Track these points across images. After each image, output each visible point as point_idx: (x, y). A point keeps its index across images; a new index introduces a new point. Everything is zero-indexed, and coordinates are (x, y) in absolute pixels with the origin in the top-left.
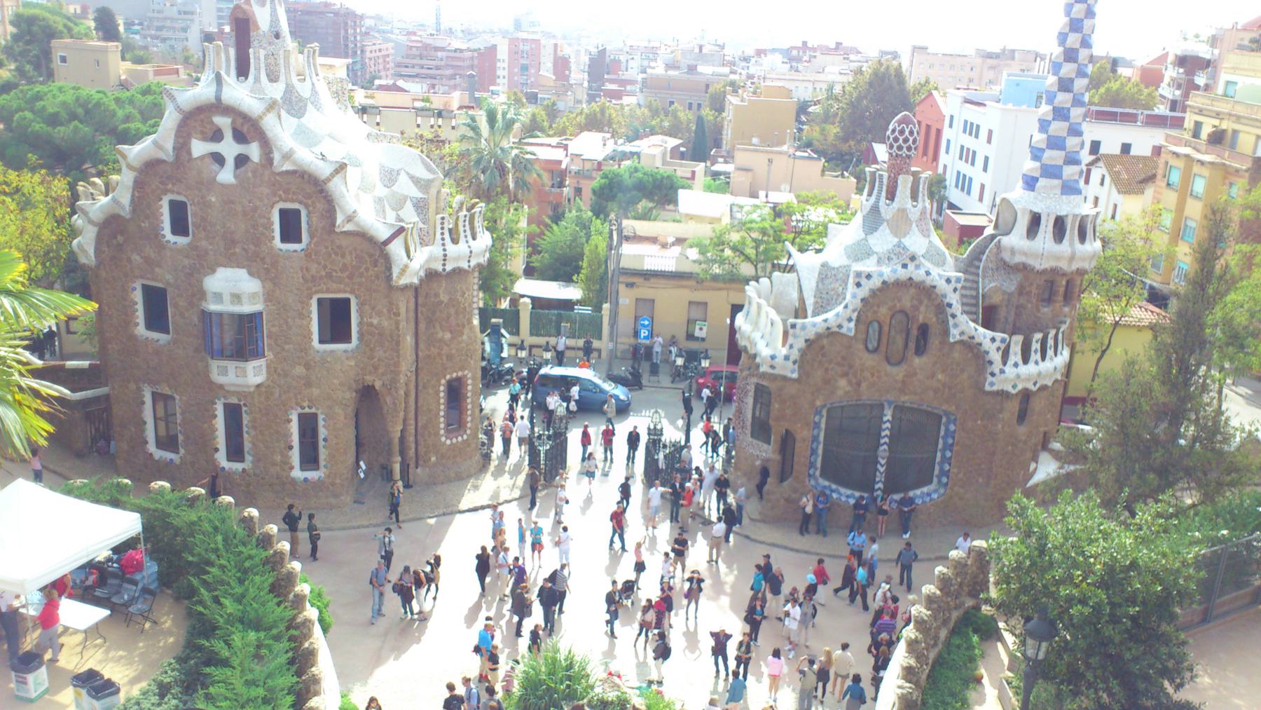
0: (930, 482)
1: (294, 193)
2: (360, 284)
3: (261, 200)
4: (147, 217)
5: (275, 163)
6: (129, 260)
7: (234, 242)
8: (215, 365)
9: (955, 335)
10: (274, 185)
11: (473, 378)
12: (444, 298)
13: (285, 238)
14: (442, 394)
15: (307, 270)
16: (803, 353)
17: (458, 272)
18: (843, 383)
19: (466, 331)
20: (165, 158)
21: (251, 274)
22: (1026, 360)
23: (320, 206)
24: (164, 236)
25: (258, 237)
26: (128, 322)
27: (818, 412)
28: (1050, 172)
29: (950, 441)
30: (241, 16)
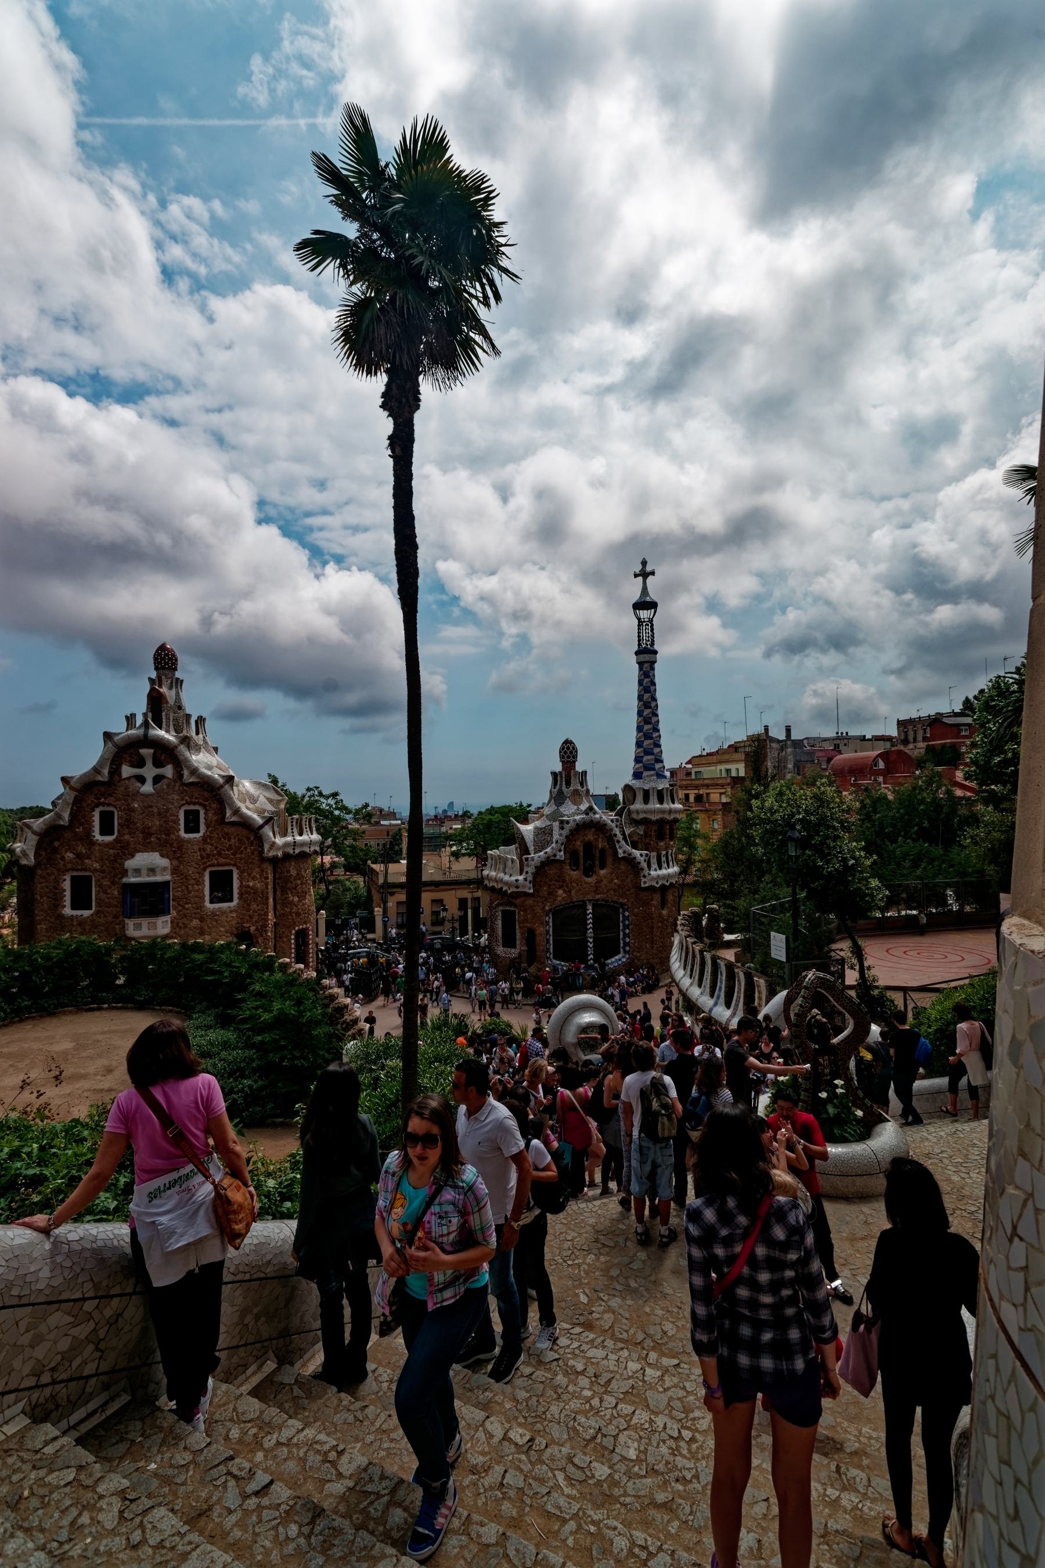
0: (619, 953)
2: (241, 859)
3: (172, 804)
4: (82, 824)
6: (63, 858)
8: (130, 923)
9: (621, 854)
12: (293, 872)
13: (186, 832)
15: (204, 850)
16: (535, 875)
18: (560, 892)
20: (101, 779)
21: (162, 856)
22: (660, 868)
25: (169, 829)
27: (547, 915)
28: (647, 768)
29: (627, 922)
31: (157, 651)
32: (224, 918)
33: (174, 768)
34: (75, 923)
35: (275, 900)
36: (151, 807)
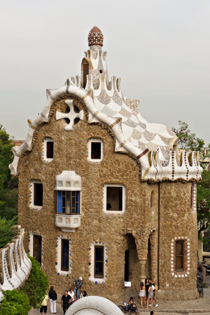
1: (98, 134)
2: (127, 179)
3: (83, 138)
4: (37, 150)
5: (89, 119)
7: (70, 158)
10: (89, 130)
11: (191, 243)
12: (174, 194)
13: (93, 157)
14: (172, 248)
15: (102, 171)
17: (180, 181)
19: (186, 215)
21: (77, 173)
23: (109, 140)
24: (43, 158)
26: (27, 202)
30: (85, 63)
31: (90, 33)
32: (114, 222)
33: (84, 112)
34: (34, 214)
35: (159, 213)
36: (71, 139)
